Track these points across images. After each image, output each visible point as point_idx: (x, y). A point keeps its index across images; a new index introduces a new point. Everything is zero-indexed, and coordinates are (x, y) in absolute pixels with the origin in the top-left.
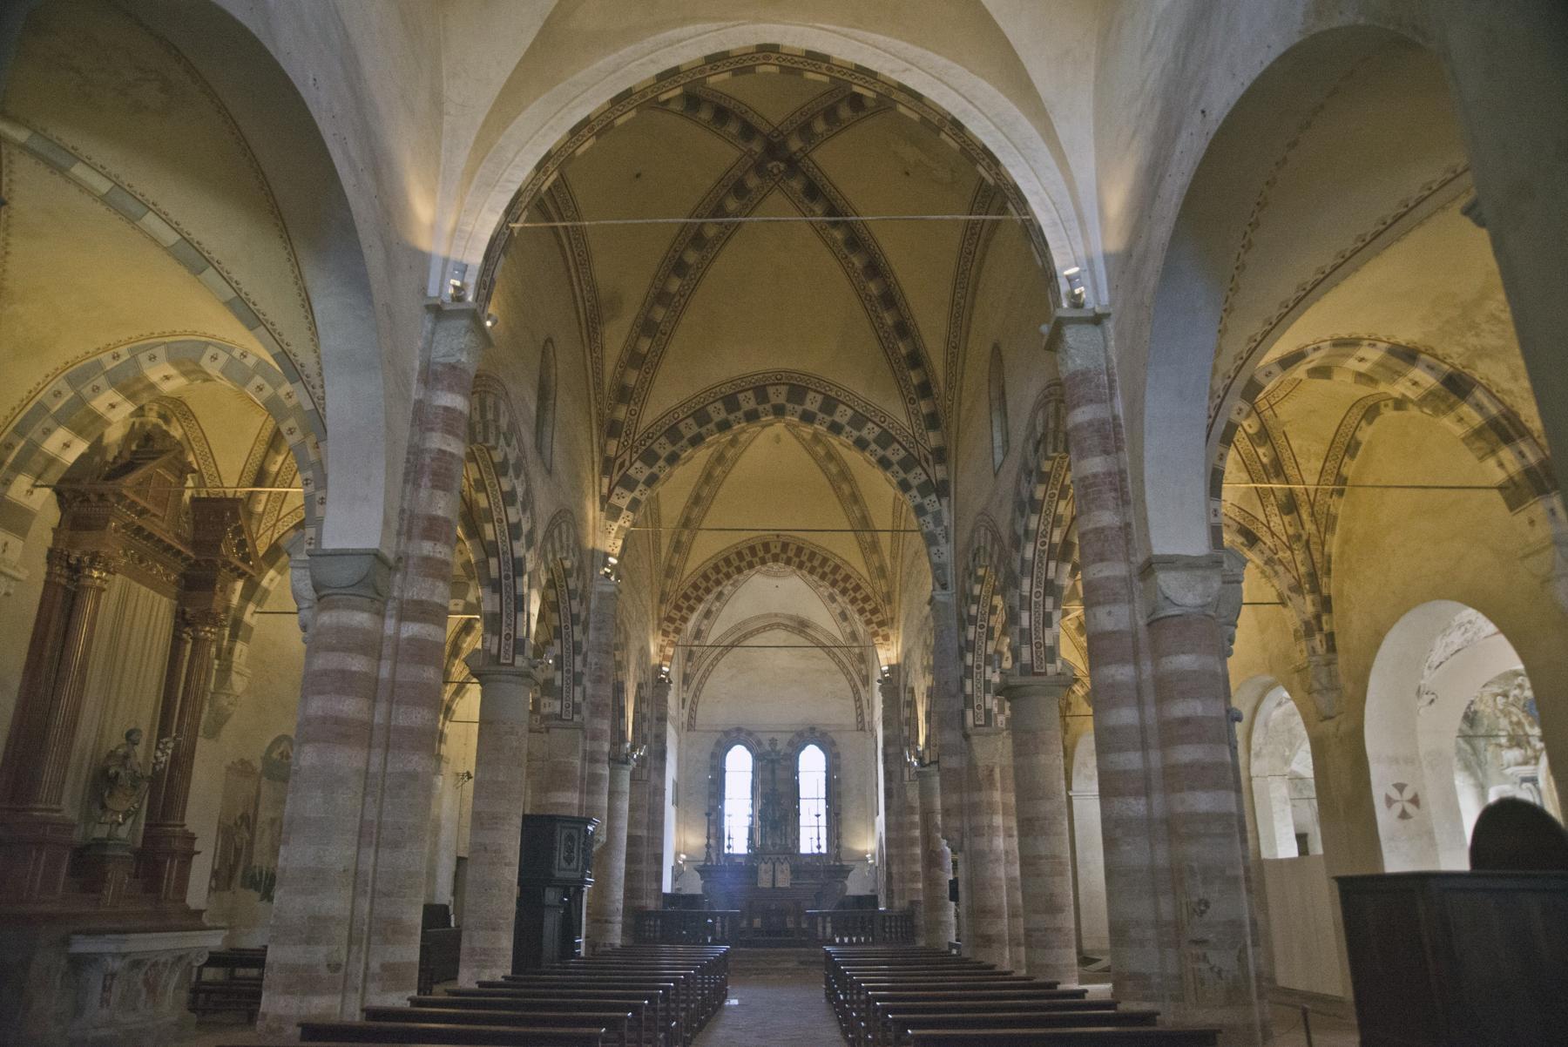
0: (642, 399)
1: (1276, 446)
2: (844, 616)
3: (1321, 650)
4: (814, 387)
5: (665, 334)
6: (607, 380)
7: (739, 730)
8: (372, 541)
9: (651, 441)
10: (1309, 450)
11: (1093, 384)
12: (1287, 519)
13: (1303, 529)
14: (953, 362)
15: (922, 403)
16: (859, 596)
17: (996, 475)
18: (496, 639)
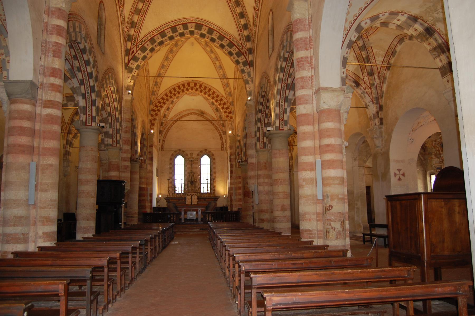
0: (140, 27)
1: (368, 51)
2: (217, 110)
3: (378, 124)
4: (205, 24)
5: (148, 1)
6: (126, 20)
7: (180, 150)
8: (29, 76)
9: (144, 43)
10: (379, 53)
11: (303, 24)
12: (370, 78)
13: (375, 81)
14: (256, 16)
15: (244, 31)
16: (222, 103)
17: (269, 58)
18: (85, 116)
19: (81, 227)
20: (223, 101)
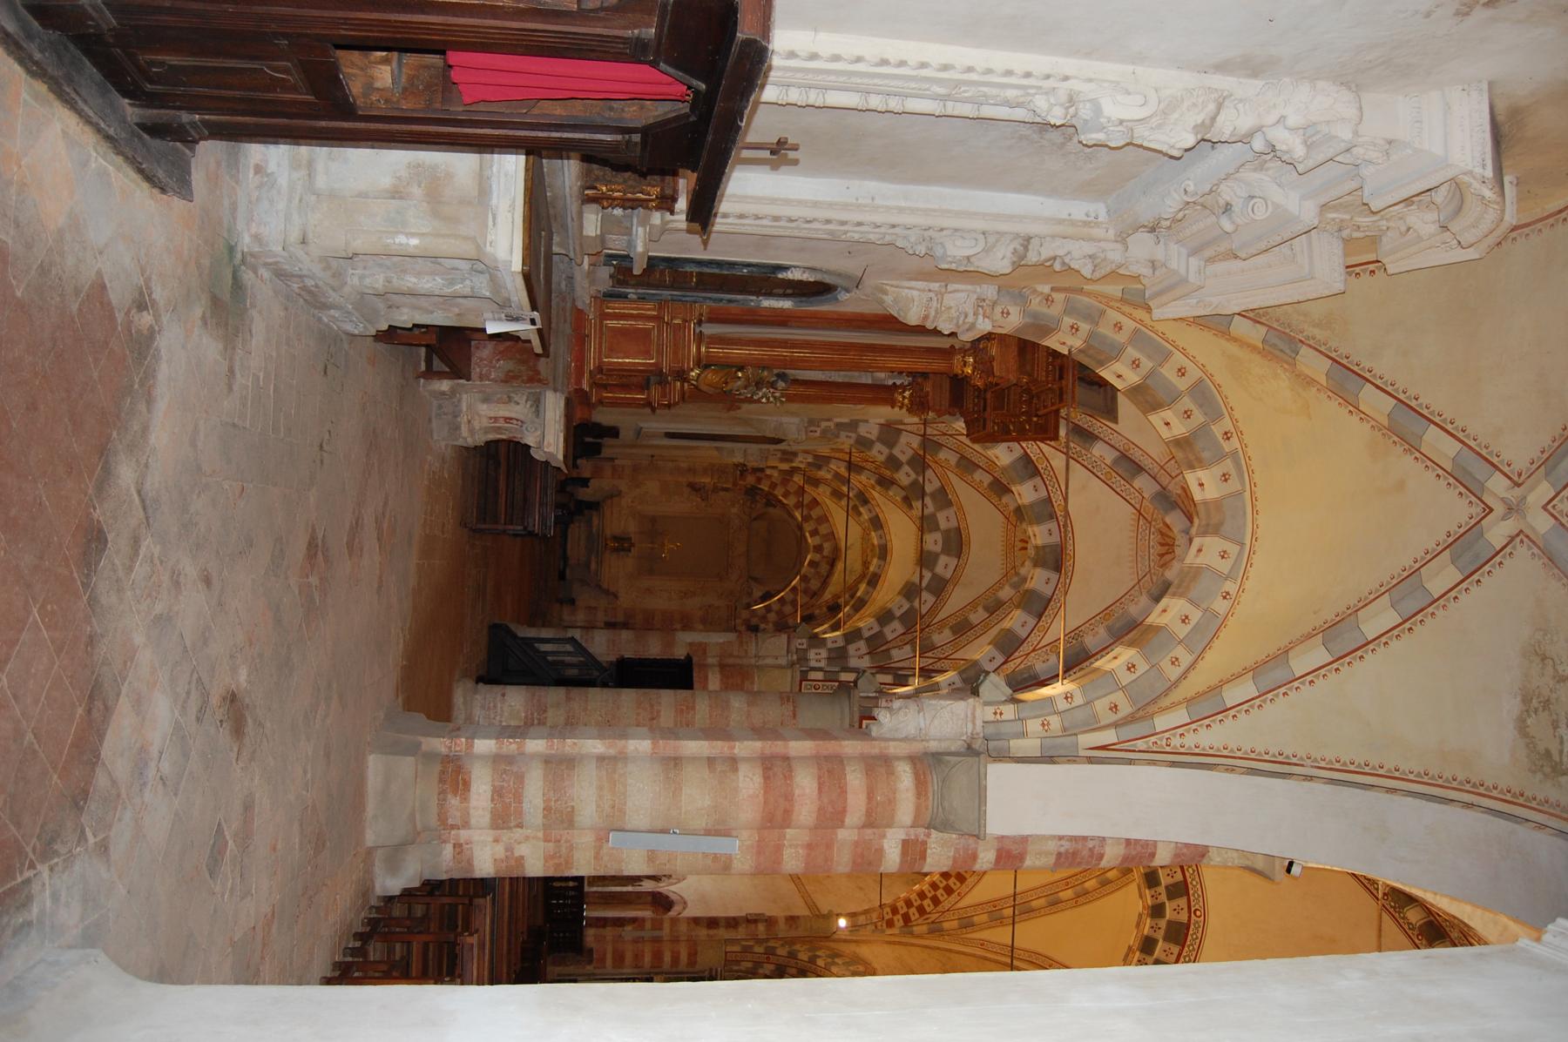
4: (1184, 954)
16: (940, 893)
19: (545, 711)
20: (946, 896)
